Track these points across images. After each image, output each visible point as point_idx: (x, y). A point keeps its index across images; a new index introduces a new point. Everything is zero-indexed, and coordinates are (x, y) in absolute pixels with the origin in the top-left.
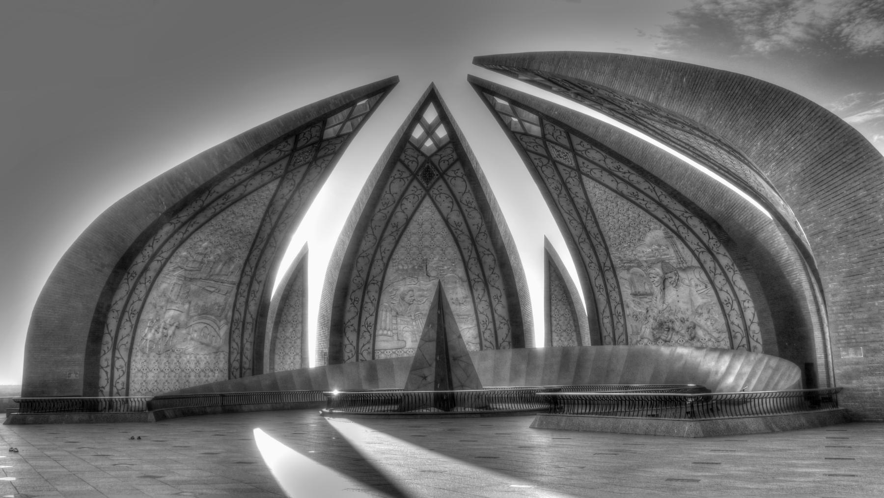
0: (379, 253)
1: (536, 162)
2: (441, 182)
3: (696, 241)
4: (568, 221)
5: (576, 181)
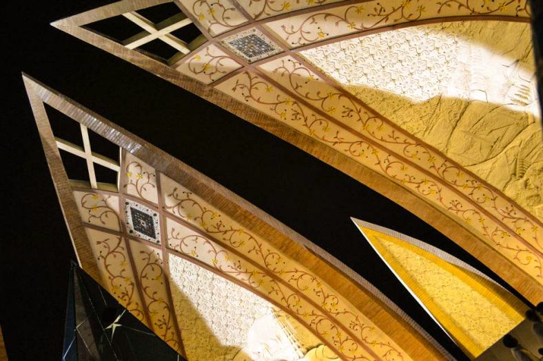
3: (310, 308)
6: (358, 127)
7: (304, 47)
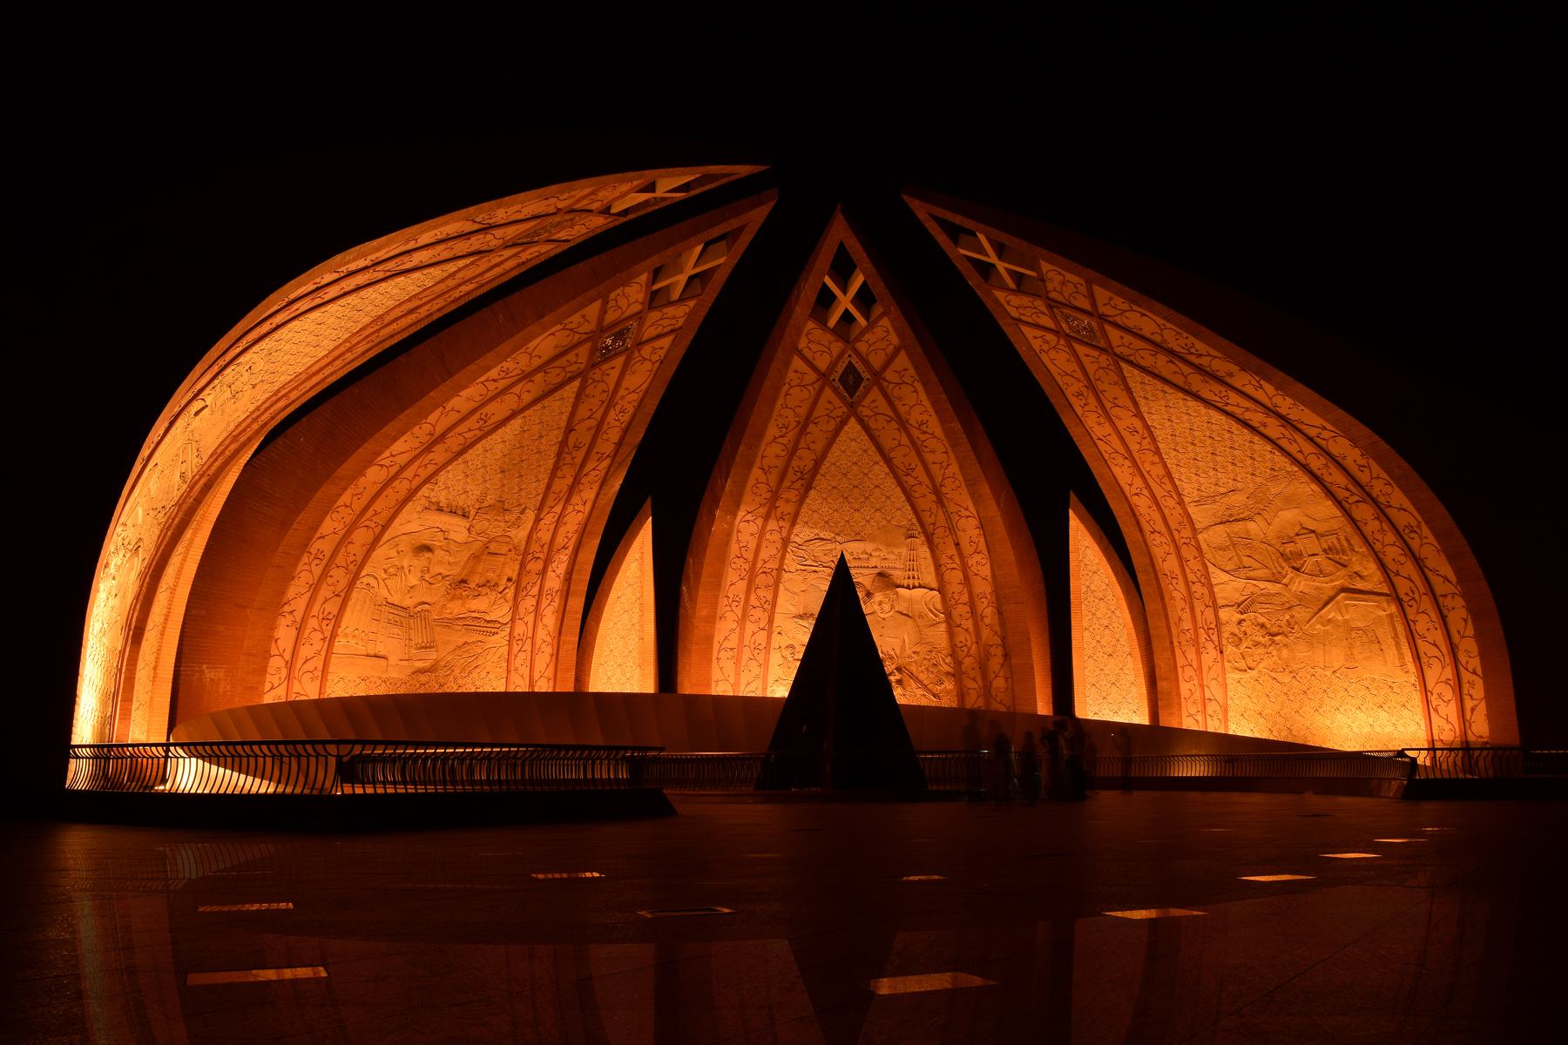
0: (417, 463)
1: (791, 375)
2: (619, 362)
4: (751, 481)
5: (832, 425)
6: (1134, 447)
7: (1131, 363)
